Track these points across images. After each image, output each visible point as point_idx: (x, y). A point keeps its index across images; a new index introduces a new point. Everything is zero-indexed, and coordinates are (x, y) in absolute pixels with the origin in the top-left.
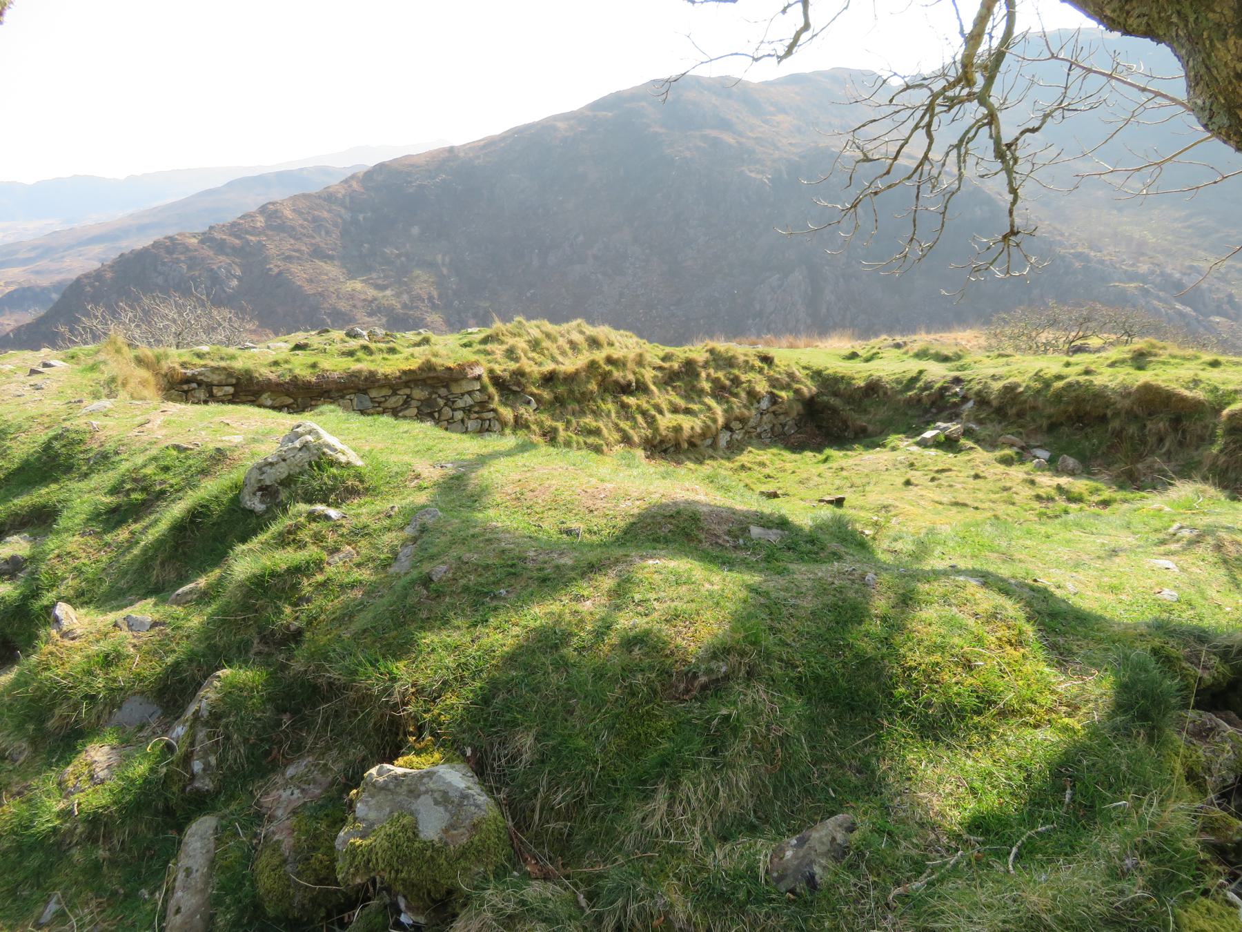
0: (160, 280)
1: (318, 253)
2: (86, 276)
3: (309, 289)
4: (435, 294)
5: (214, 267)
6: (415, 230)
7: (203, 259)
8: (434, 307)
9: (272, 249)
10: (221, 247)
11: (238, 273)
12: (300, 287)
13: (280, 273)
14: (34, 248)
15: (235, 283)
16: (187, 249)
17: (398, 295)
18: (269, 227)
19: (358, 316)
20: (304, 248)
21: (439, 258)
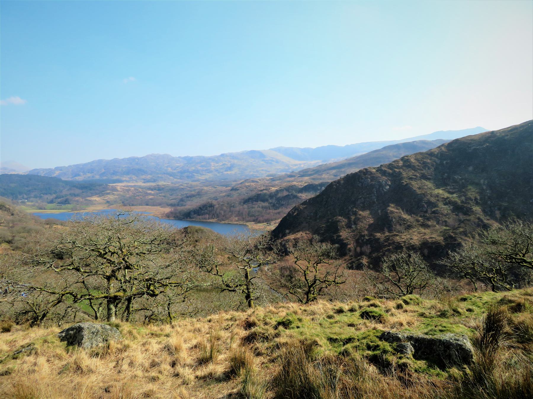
0: (360, 185)
1: (424, 177)
2: (335, 182)
3: (419, 192)
4: (478, 197)
5: (381, 181)
6: (471, 168)
7: (377, 178)
8: (477, 203)
9: (404, 174)
10: (384, 173)
11: (390, 183)
12: (415, 190)
13: (407, 184)
14: (314, 170)
15: (388, 187)
16: (371, 173)
17: (459, 197)
18: (404, 166)
19: (440, 205)
20: (418, 175)
21: (482, 181)
